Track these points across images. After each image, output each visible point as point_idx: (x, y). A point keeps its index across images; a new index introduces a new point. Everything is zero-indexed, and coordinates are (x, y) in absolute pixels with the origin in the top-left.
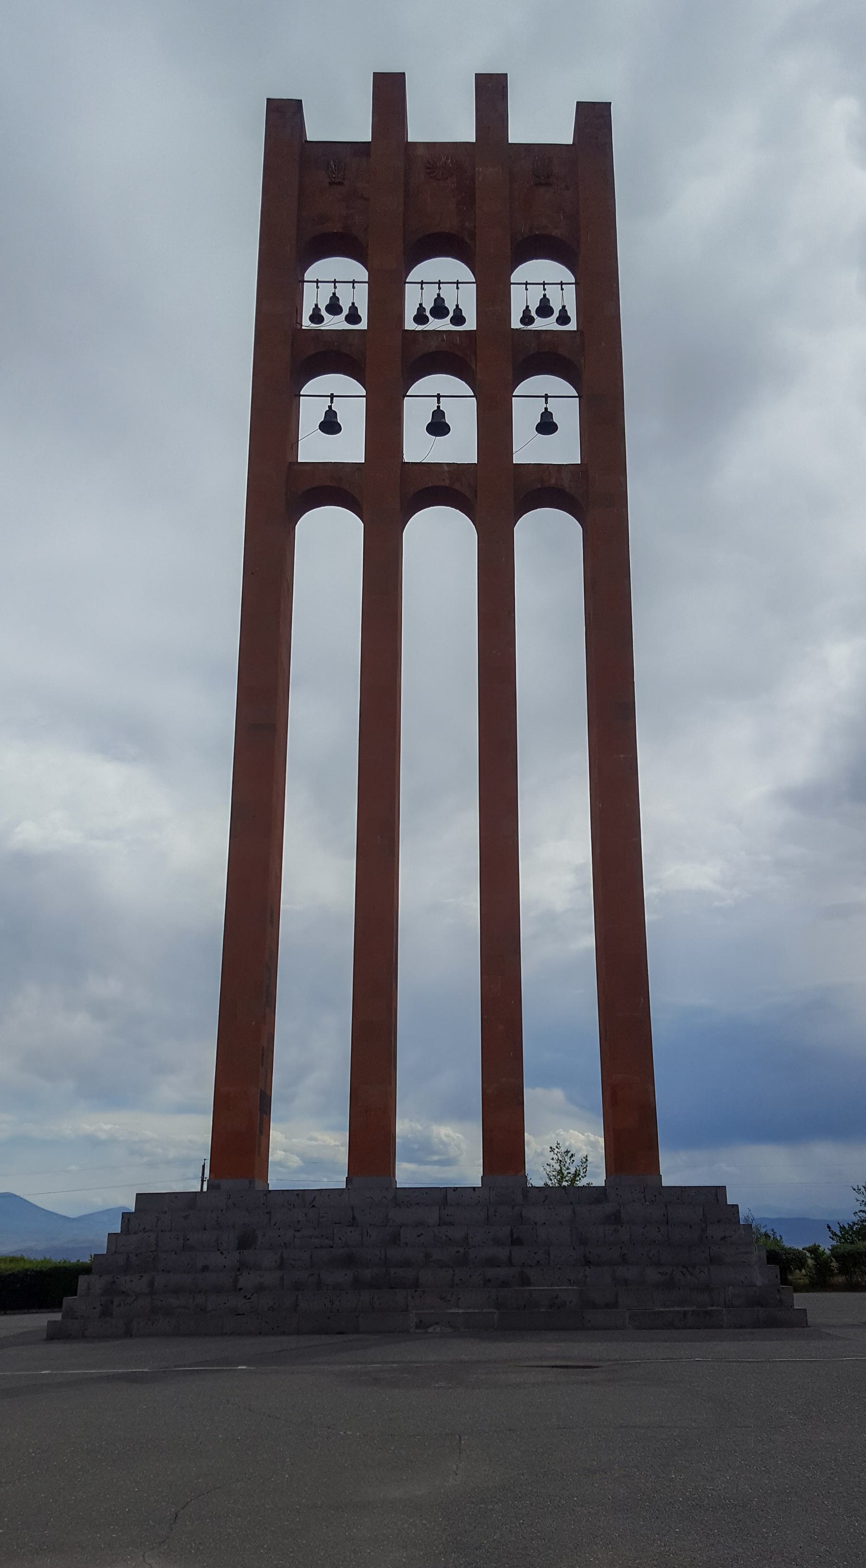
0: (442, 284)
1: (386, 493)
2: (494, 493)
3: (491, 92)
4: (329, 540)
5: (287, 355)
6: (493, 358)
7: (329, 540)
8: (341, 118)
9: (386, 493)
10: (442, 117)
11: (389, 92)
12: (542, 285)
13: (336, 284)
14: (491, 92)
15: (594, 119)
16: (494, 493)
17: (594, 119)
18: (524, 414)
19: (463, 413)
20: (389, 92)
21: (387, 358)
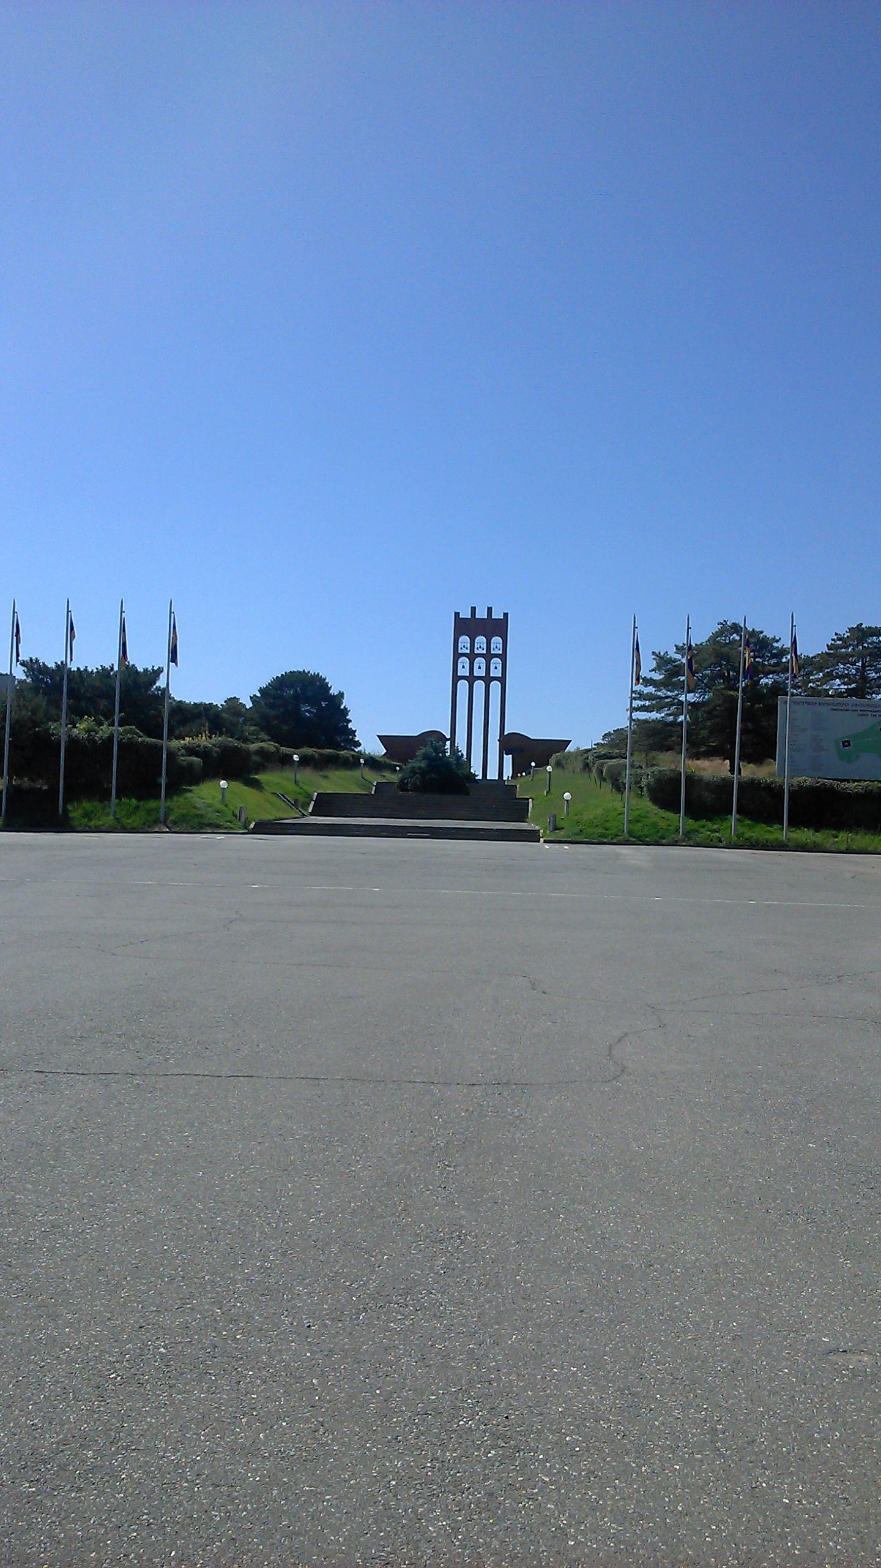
0: (481, 640)
1: (471, 679)
2: (488, 679)
3: (490, 610)
4: (463, 685)
5: (457, 656)
6: (488, 657)
7: (463, 685)
8: (466, 614)
9: (471, 679)
10: (482, 614)
11: (473, 609)
12: (497, 641)
13: (465, 640)
14: (490, 610)
15: (506, 615)
16: (488, 679)
17: (506, 615)
18: (492, 667)
19: (484, 667)
20: (473, 609)
21: (472, 656)
